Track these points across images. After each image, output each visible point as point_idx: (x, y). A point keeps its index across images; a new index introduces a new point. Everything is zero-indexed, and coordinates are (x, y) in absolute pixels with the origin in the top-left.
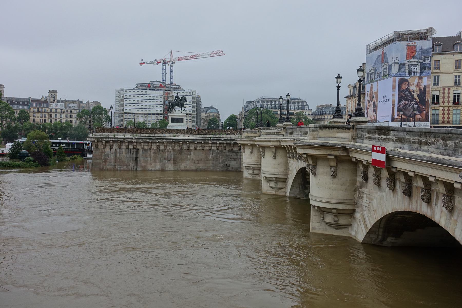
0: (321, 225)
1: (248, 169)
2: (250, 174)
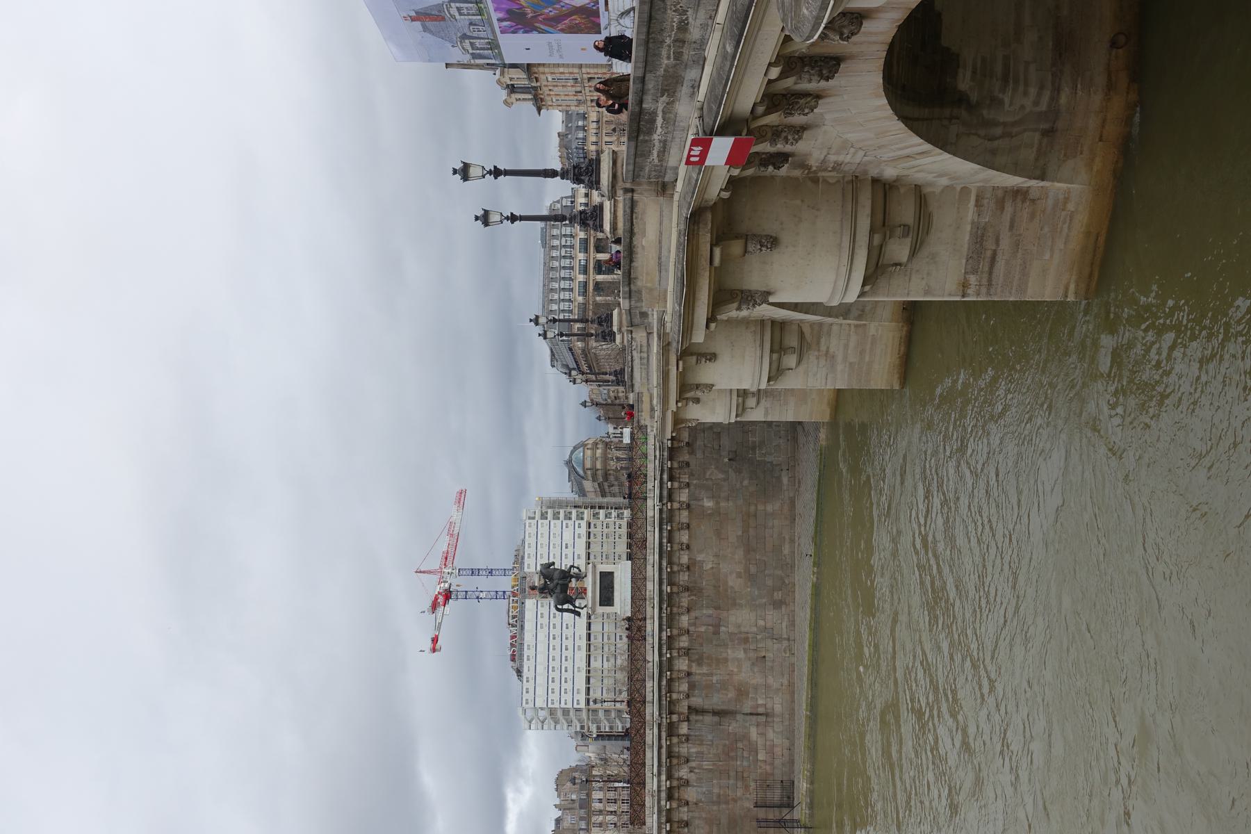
0: (918, 271)
1: (744, 409)
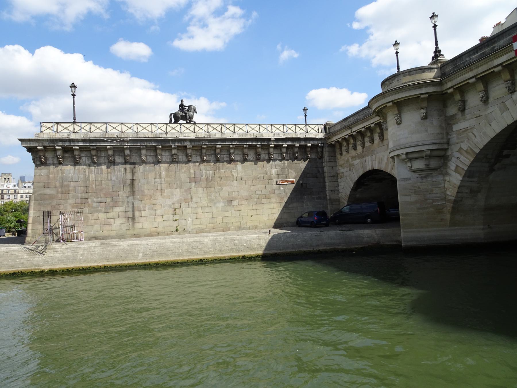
2: (415, 171)
